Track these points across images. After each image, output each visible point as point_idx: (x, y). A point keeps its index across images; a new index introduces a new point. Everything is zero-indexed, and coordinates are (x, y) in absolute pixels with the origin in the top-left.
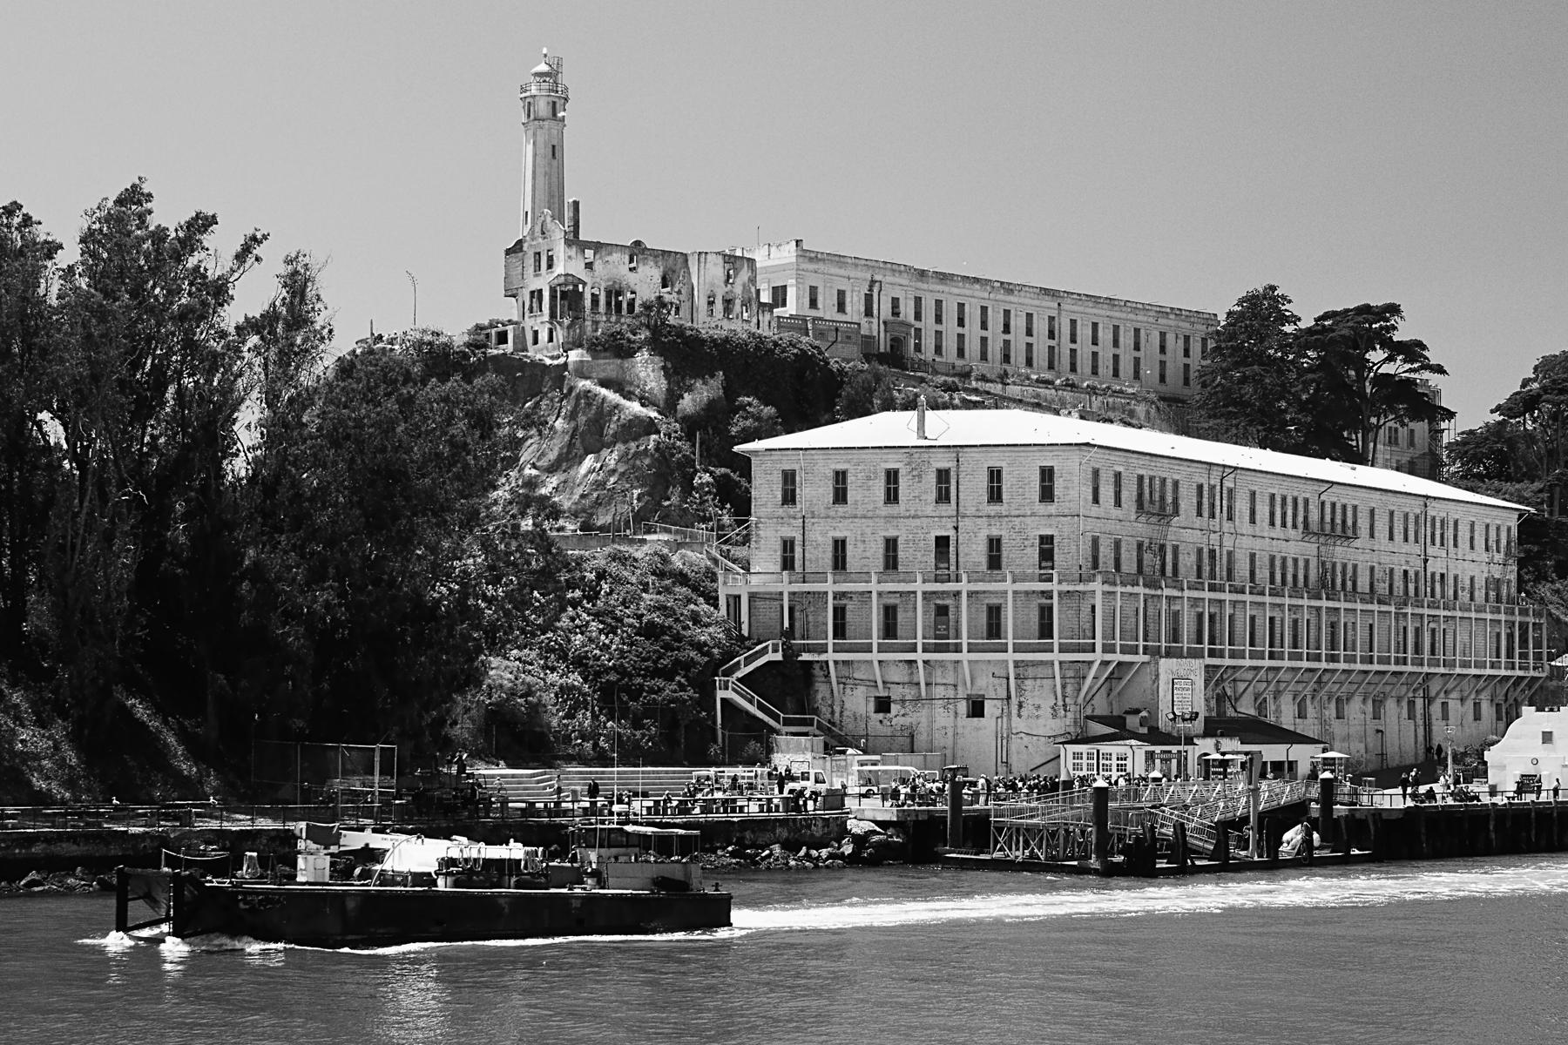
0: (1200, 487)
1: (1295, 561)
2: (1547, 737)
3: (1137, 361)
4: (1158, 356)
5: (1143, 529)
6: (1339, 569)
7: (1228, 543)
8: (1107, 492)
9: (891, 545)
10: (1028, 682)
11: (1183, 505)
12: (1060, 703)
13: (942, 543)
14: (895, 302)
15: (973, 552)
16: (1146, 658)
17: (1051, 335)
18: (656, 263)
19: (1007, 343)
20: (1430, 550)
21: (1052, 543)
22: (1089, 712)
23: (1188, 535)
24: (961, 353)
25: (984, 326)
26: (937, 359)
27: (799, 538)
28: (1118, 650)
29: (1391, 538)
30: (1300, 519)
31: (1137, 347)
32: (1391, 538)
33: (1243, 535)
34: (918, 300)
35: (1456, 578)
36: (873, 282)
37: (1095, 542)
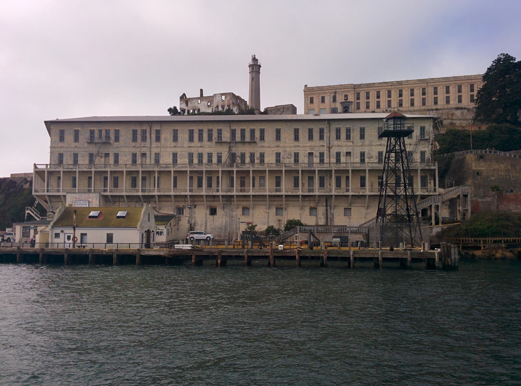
0: (135, 132)
1: (210, 156)
8: (69, 137)
11: (121, 138)
14: (346, 96)
17: (424, 94)
23: (127, 150)
25: (389, 96)
29: (297, 138)
32: (297, 138)
33: (167, 147)
35: (362, 155)
36: (335, 93)
37: (61, 156)
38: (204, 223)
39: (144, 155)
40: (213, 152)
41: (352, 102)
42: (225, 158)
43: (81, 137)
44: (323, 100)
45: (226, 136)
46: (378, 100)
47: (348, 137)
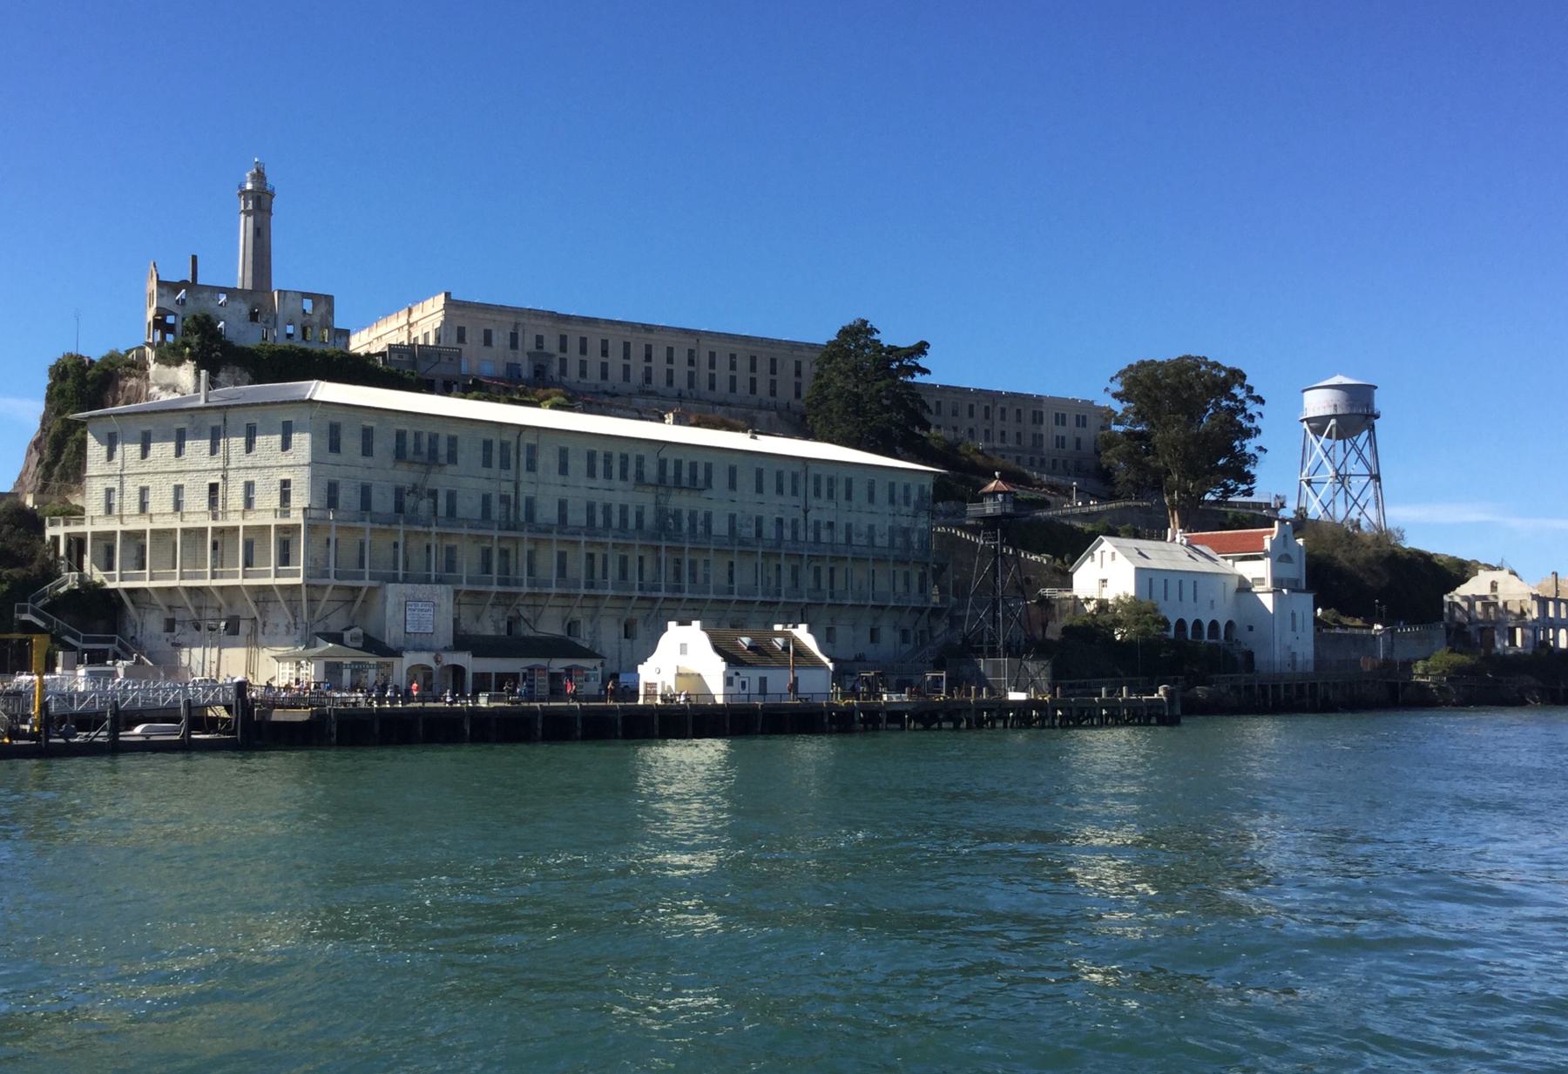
2: (683, 649)
3: (773, 383)
4: (793, 379)
5: (405, 476)
6: (685, 515)
7: (526, 491)
8: (351, 443)
9: (178, 490)
10: (270, 604)
11: (461, 457)
12: (292, 622)
13: (213, 488)
14: (539, 339)
15: (234, 497)
16: (374, 584)
17: (691, 362)
18: (244, 299)
19: (648, 370)
20: (813, 502)
21: (289, 486)
22: (320, 628)
24: (604, 375)
26: (582, 381)
27: (117, 487)
28: (464, 581)
29: (759, 489)
30: (632, 470)
31: (773, 371)
32: (759, 489)
34: (563, 339)
35: (848, 527)
36: (516, 325)
37: (333, 489)
38: (617, 653)
39: (504, 499)
40: (630, 504)
41: (552, 356)
42: (649, 519)
43: (377, 446)
44: (488, 339)
45: (651, 470)
46: (604, 359)
47: (830, 495)
